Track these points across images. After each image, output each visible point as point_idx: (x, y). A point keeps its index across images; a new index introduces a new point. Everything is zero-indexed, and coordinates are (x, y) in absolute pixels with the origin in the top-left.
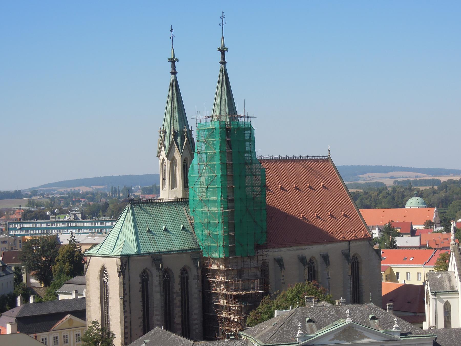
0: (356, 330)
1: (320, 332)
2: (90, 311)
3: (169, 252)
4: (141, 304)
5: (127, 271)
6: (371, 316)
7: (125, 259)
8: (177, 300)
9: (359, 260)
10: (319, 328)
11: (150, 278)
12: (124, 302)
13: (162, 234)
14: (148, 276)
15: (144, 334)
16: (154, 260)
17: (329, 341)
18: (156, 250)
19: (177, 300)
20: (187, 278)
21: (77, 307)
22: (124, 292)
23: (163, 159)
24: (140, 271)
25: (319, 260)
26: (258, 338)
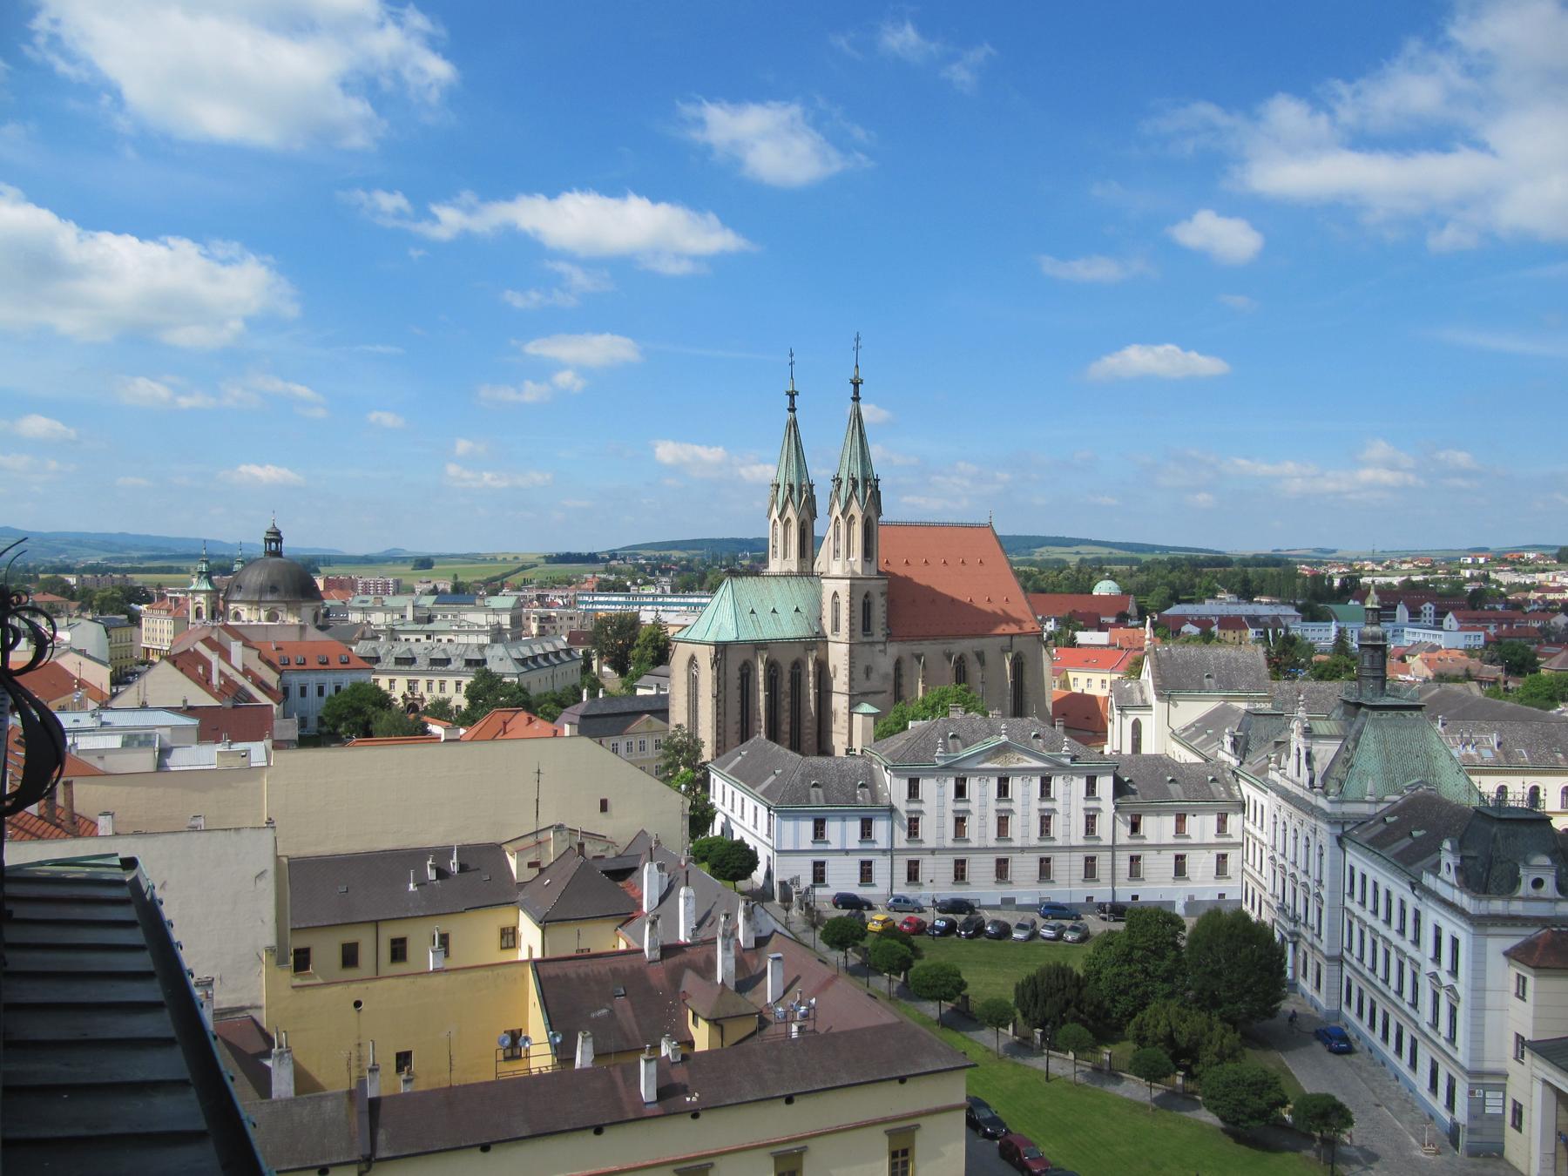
1: (966, 750)
2: (673, 712)
4: (739, 705)
6: (1033, 734)
7: (722, 647)
8: (786, 703)
9: (1024, 660)
10: (966, 746)
11: (752, 673)
12: (717, 701)
13: (769, 616)
14: (749, 669)
15: (742, 743)
19: (786, 703)
20: (800, 674)
21: (658, 706)
24: (739, 663)
25: (972, 658)
26: (886, 756)
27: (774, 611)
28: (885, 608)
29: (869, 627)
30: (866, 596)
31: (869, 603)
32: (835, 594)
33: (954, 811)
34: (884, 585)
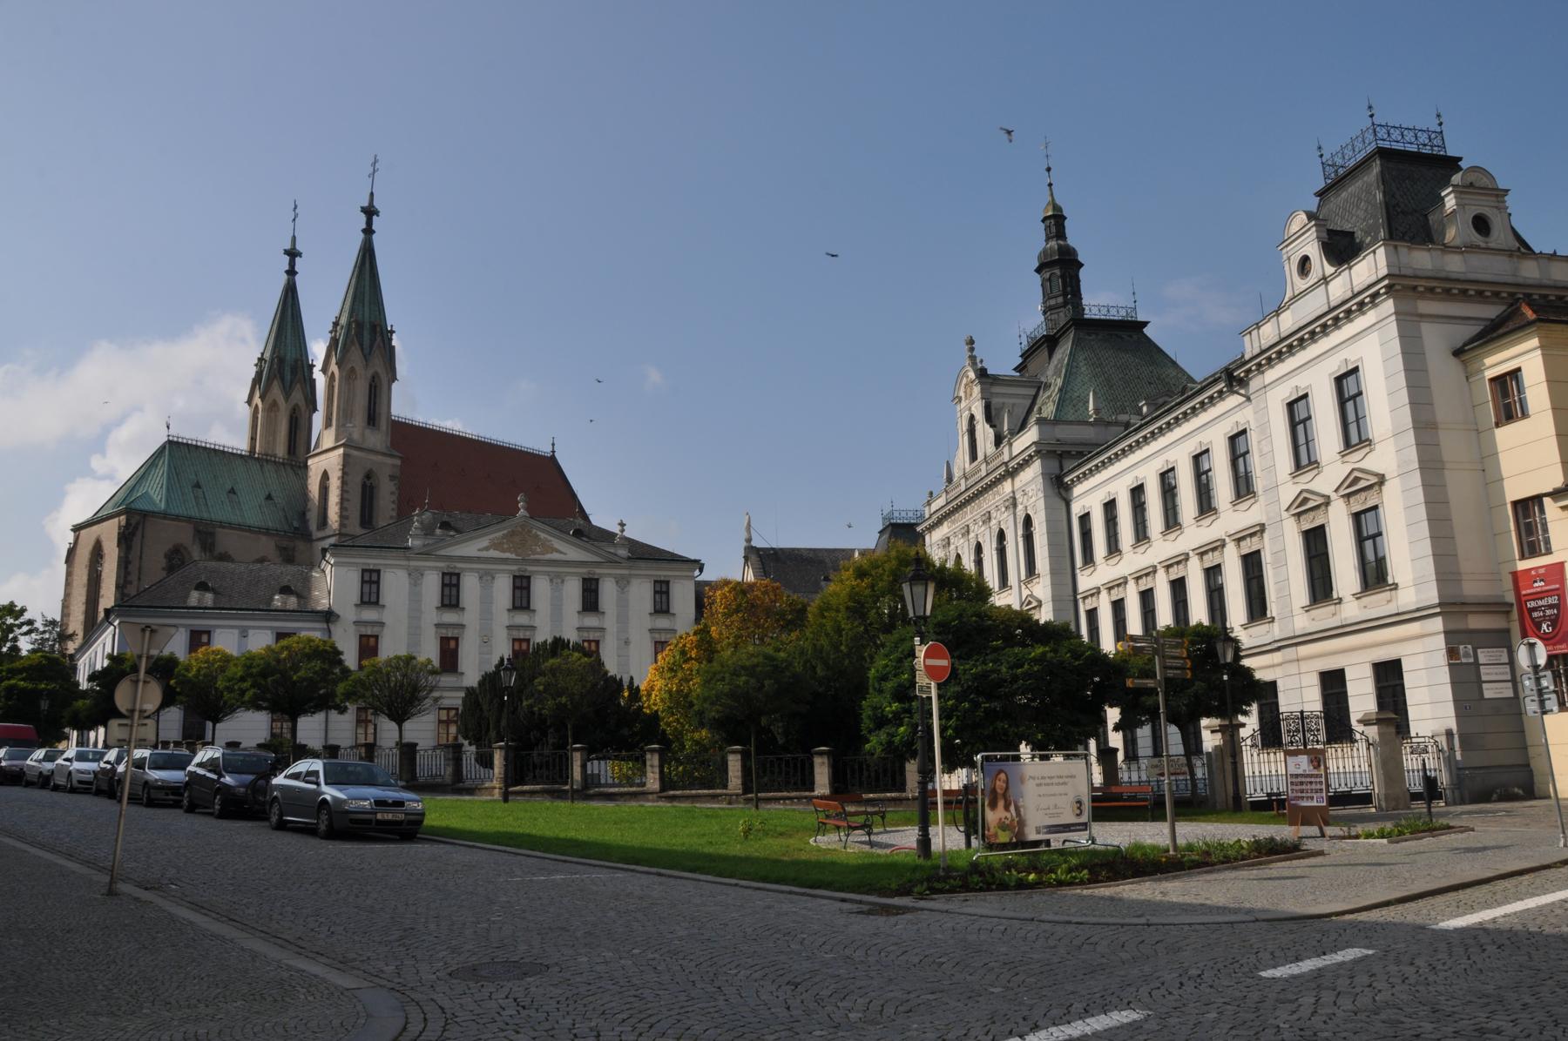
0: (538, 536)
3: (231, 526)
5: (137, 540)
7: (137, 518)
16: (199, 532)
17: (479, 550)
18: (205, 516)
22: (125, 577)
23: (257, 405)
27: (232, 491)
28: (394, 498)
29: (371, 517)
30: (368, 476)
31: (372, 488)
32: (325, 476)
33: (438, 626)
34: (394, 466)
